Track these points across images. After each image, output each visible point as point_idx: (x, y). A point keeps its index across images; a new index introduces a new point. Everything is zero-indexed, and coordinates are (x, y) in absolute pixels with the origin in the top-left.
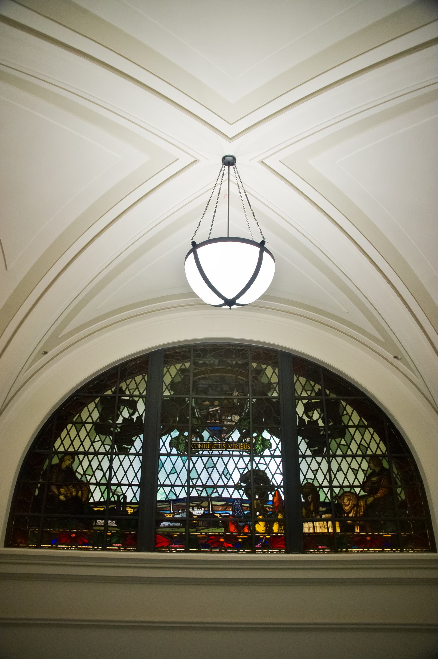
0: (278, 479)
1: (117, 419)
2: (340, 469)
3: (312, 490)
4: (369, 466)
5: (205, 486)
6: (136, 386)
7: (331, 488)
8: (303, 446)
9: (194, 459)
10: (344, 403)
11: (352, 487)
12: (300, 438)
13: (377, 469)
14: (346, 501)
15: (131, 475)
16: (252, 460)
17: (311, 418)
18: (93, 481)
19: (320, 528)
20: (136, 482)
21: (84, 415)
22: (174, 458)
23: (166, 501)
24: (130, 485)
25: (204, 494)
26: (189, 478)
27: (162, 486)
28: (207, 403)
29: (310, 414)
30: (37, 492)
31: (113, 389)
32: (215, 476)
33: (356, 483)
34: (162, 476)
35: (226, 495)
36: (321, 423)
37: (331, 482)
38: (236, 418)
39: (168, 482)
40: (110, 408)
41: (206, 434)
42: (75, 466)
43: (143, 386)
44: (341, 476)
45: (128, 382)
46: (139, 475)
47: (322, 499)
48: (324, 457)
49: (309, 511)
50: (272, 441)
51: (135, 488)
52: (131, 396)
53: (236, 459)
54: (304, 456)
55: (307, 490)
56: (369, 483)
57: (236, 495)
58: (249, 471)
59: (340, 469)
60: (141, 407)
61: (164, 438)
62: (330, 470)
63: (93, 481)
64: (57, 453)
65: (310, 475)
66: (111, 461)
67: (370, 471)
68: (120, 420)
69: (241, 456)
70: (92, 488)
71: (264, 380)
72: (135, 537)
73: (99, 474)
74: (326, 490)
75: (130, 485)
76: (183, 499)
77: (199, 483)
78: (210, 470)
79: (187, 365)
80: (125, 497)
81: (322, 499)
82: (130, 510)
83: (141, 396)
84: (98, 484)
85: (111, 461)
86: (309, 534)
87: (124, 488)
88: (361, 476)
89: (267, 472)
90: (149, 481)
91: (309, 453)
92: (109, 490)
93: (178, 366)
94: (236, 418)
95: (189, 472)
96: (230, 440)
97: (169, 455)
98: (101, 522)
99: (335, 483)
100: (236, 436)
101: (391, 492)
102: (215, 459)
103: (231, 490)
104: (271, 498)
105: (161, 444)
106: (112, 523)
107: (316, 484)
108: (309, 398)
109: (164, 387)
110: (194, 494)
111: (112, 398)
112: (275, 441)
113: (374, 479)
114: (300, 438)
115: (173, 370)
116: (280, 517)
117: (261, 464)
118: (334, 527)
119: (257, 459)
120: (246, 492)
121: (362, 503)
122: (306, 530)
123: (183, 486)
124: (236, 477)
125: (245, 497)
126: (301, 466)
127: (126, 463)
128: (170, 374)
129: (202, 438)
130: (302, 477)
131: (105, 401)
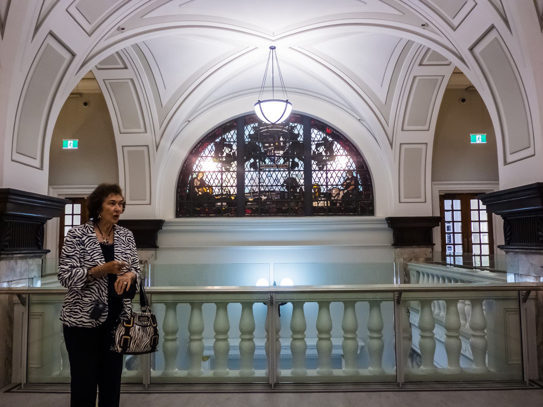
0: (302, 181)
1: (223, 153)
2: (332, 177)
3: (319, 187)
4: (346, 176)
5: (267, 186)
6: (231, 136)
7: (327, 186)
8: (314, 166)
9: (262, 173)
10: (336, 143)
11: (337, 185)
12: (313, 161)
13: (350, 177)
14: (334, 191)
15: (232, 181)
16: (289, 173)
17: (318, 151)
18: (214, 185)
19: (321, 204)
20: (234, 185)
21: (207, 152)
22: (252, 173)
23: (250, 193)
24: (232, 186)
25: (267, 190)
26: (259, 182)
27: (247, 186)
28: (267, 145)
29: (318, 149)
30: (188, 191)
31: (220, 138)
32: (272, 181)
33: (339, 183)
34: (247, 182)
35: (277, 189)
36: (324, 154)
37: (327, 183)
38: (281, 152)
39: (249, 184)
40: (220, 147)
41: (267, 161)
42: (204, 178)
43: (235, 137)
44: (332, 180)
45: (227, 134)
46: (236, 181)
47: (322, 191)
48: (324, 171)
49: (316, 197)
50: (299, 163)
51: (234, 188)
52: (230, 142)
53: (282, 172)
54: (315, 171)
55: (315, 187)
56: (345, 184)
57: (282, 190)
58: (288, 178)
59: (332, 177)
60: (235, 147)
61: (247, 163)
62: (327, 177)
63: (214, 185)
64: (195, 172)
65: (317, 180)
66: (222, 175)
67: (346, 178)
68: (225, 155)
69: (284, 171)
70: (214, 188)
71: (296, 132)
72: (235, 210)
73: (217, 181)
74: (324, 187)
75: (232, 186)
76: (257, 192)
77: (264, 184)
78: (269, 178)
79: (257, 124)
80: (230, 192)
81: (322, 191)
82: (233, 198)
83: (234, 142)
84: (216, 186)
85: (222, 175)
86: (315, 207)
87: (229, 188)
88: (342, 180)
89: (297, 178)
90: (241, 185)
91: (317, 169)
92: (222, 189)
93: (252, 125)
94: (281, 152)
95: (259, 179)
96: (279, 163)
97: (249, 171)
98: (219, 204)
99: (329, 183)
100: (282, 161)
101: (356, 188)
102: (272, 173)
103: (279, 187)
104: (298, 191)
105: (245, 166)
106: (224, 204)
107: (320, 184)
108: (319, 141)
109: (245, 137)
110: (262, 189)
111: (220, 142)
112: (301, 163)
113: (348, 181)
114: (313, 161)
115: (249, 127)
116: (302, 199)
117: (294, 174)
118: (327, 204)
119: (292, 172)
120: (286, 188)
121: (341, 193)
122: (314, 205)
123: (257, 186)
124: (282, 181)
125: (286, 190)
126: (313, 175)
127: (229, 176)
128: (249, 130)
129: (265, 163)
130: (313, 181)
131: (216, 144)
